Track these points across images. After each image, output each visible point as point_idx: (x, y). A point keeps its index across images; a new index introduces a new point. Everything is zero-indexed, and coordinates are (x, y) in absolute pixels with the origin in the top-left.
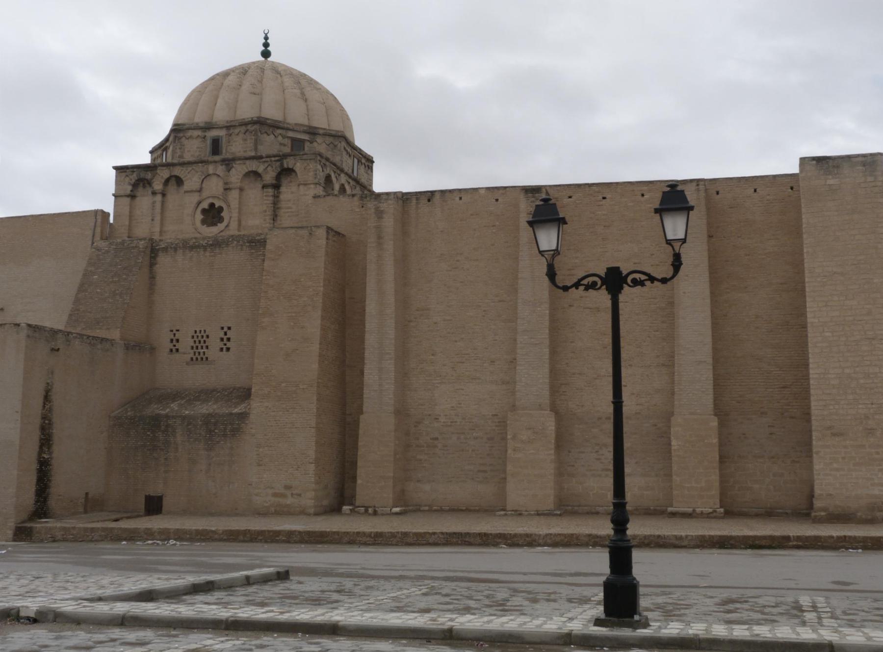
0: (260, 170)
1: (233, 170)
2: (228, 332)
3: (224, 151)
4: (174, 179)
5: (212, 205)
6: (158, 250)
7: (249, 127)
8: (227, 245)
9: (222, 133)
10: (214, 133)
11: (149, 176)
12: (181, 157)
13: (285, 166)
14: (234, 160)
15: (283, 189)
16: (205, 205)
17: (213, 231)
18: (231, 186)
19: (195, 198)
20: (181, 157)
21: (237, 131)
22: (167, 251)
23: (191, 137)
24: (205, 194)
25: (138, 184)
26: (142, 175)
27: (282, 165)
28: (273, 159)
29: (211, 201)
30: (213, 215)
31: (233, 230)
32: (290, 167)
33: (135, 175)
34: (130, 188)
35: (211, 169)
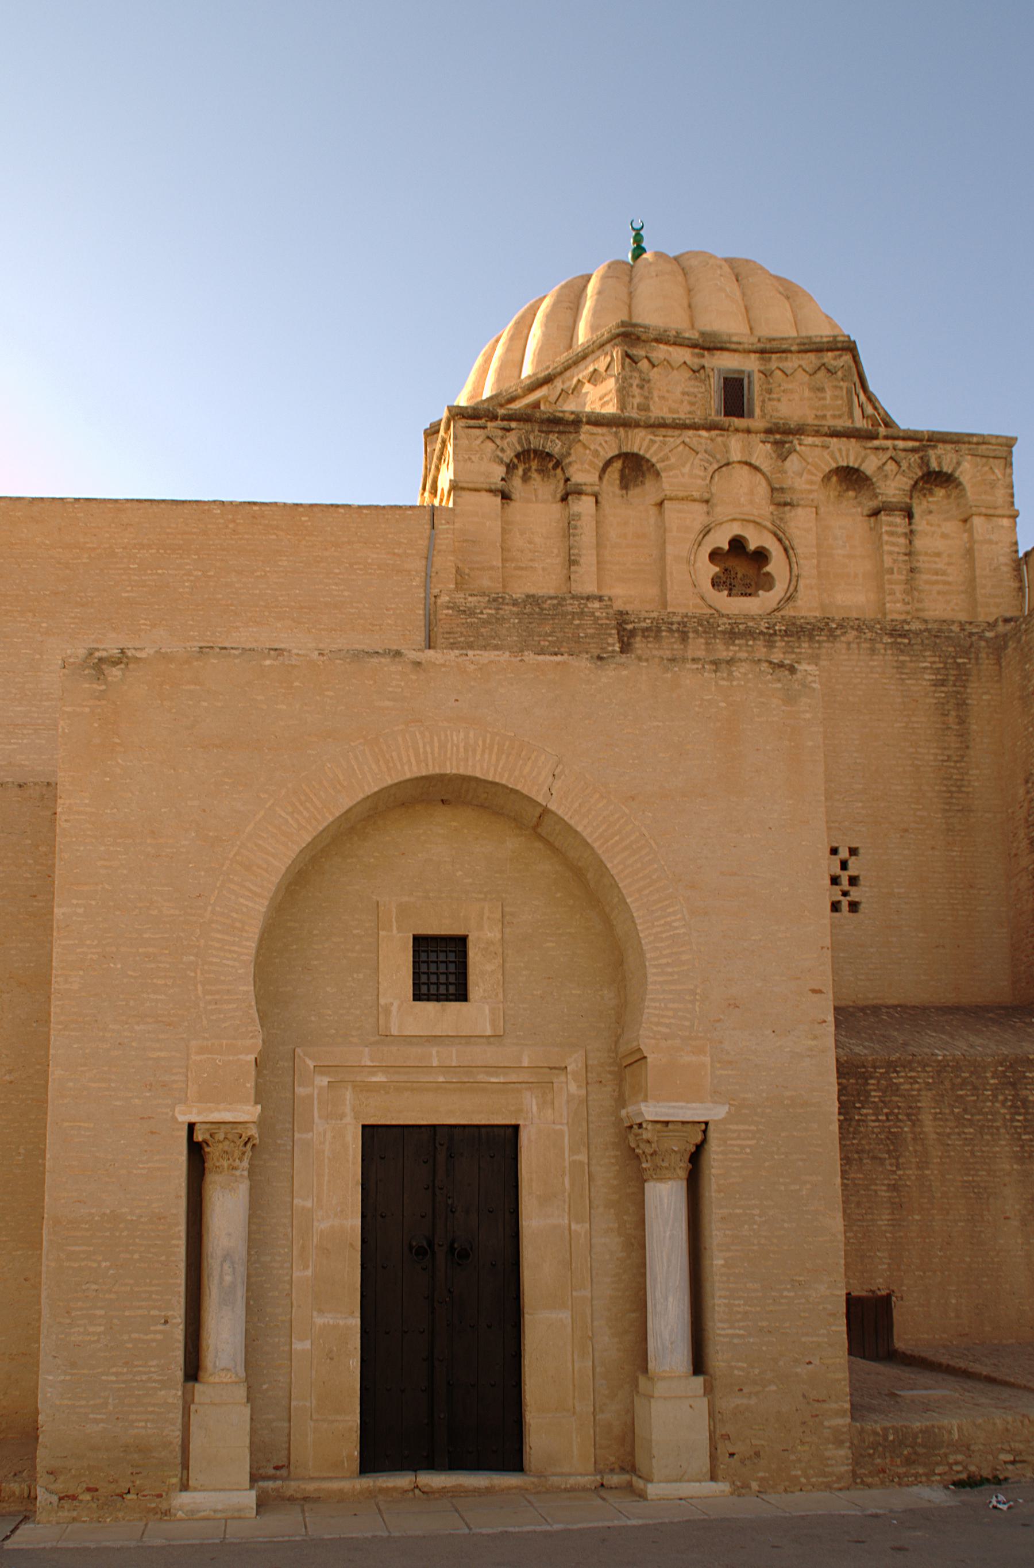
0: (870, 466)
1: (794, 457)
2: (852, 862)
3: (757, 411)
4: (618, 465)
5: (737, 544)
6: (632, 633)
7: (828, 357)
8: (832, 636)
9: (751, 364)
10: (728, 362)
11: (555, 445)
12: (644, 408)
13: (934, 465)
14: (800, 431)
15: (920, 523)
16: (721, 540)
17: (753, 606)
18: (795, 498)
19: (696, 516)
20: (644, 408)
21: (792, 363)
22: (658, 637)
23: (668, 363)
24: (721, 511)
25: (515, 467)
26: (537, 441)
27: (924, 462)
28: (900, 444)
29: (736, 529)
30: (741, 564)
31: (807, 607)
32: (947, 469)
33: (512, 437)
34: (500, 471)
35: (735, 447)
